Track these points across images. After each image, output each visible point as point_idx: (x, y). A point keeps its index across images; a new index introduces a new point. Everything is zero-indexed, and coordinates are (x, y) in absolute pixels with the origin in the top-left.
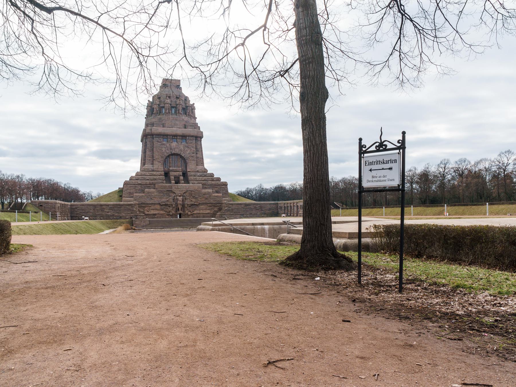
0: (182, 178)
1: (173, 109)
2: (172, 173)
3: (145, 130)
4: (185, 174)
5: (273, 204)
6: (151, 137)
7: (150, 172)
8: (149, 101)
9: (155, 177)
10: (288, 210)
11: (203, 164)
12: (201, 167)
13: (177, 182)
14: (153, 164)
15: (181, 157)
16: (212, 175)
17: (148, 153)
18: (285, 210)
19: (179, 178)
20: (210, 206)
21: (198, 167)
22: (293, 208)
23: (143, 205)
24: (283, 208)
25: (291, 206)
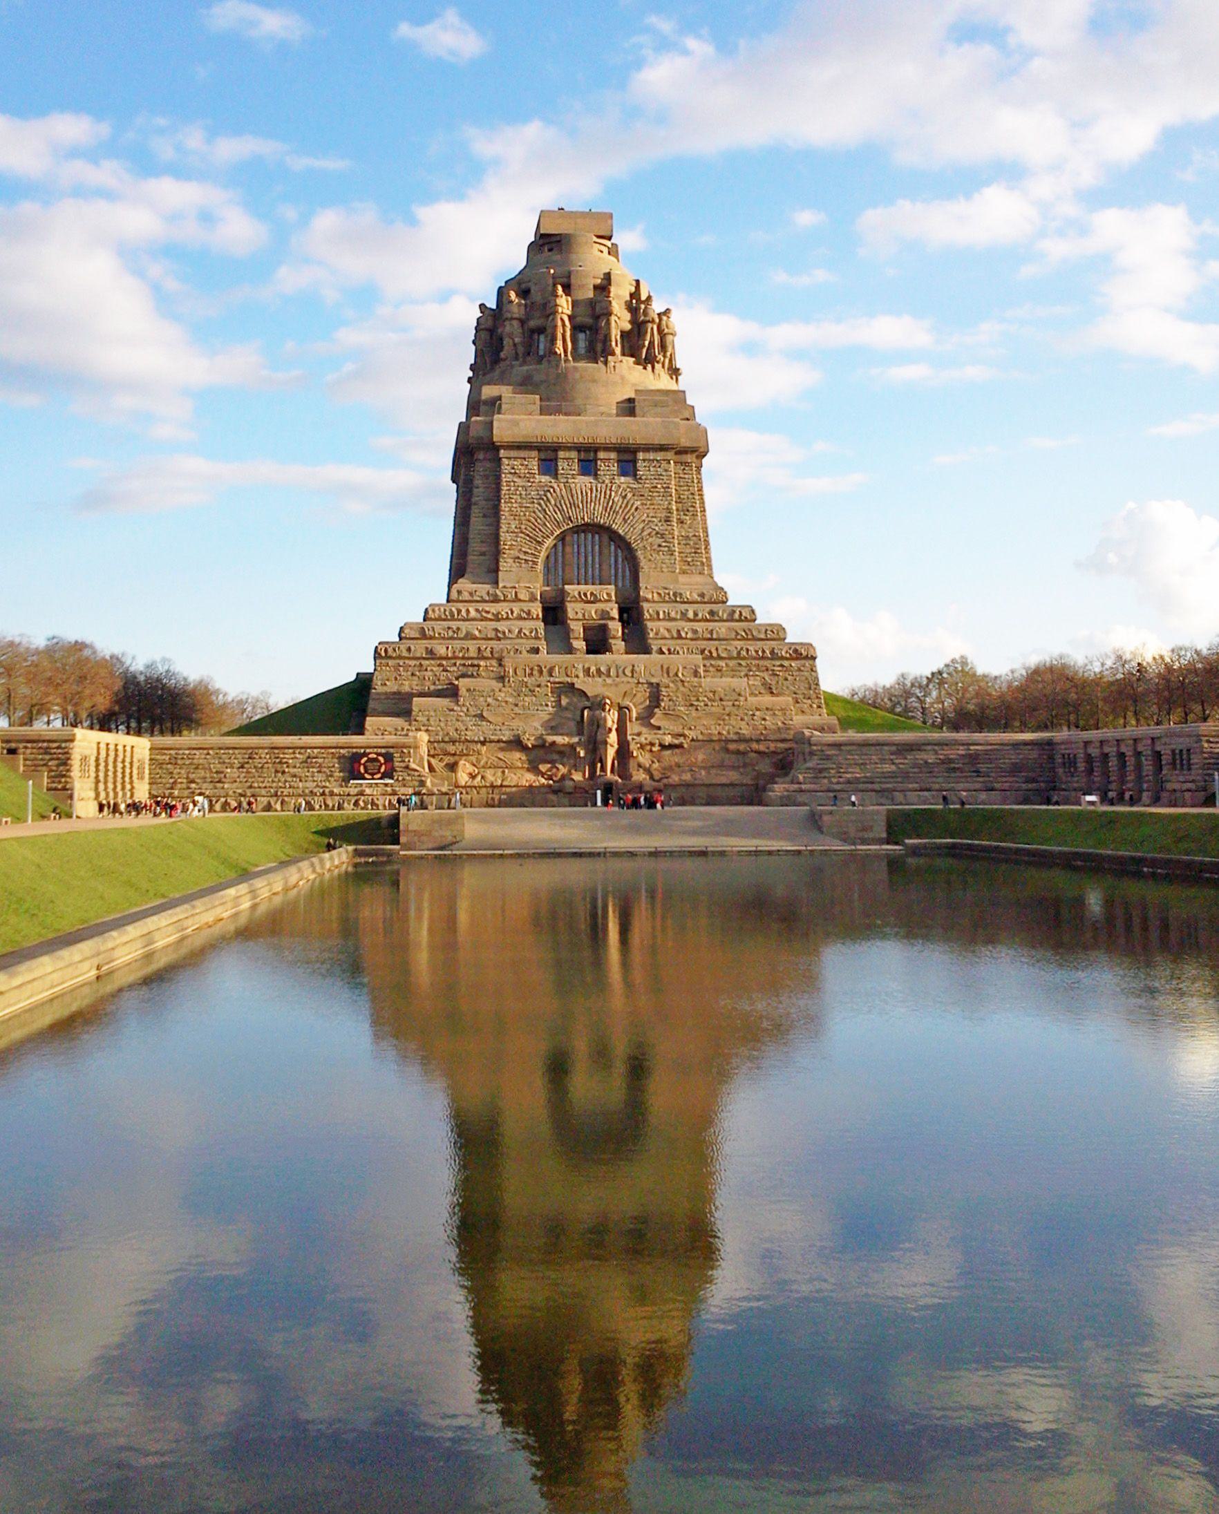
0: (616, 627)
1: (581, 336)
2: (572, 609)
3: (463, 429)
4: (631, 613)
5: (1026, 743)
6: (490, 455)
7: (487, 607)
8: (482, 307)
9: (502, 626)
10: (1106, 774)
11: (710, 567)
12: (699, 579)
13: (598, 642)
14: (497, 570)
15: (614, 537)
16: (746, 615)
17: (477, 523)
18: (1090, 771)
19: (604, 628)
20: (738, 752)
21: (682, 579)
22: (1131, 762)
23: (451, 748)
24: (1081, 766)
25: (1121, 756)
